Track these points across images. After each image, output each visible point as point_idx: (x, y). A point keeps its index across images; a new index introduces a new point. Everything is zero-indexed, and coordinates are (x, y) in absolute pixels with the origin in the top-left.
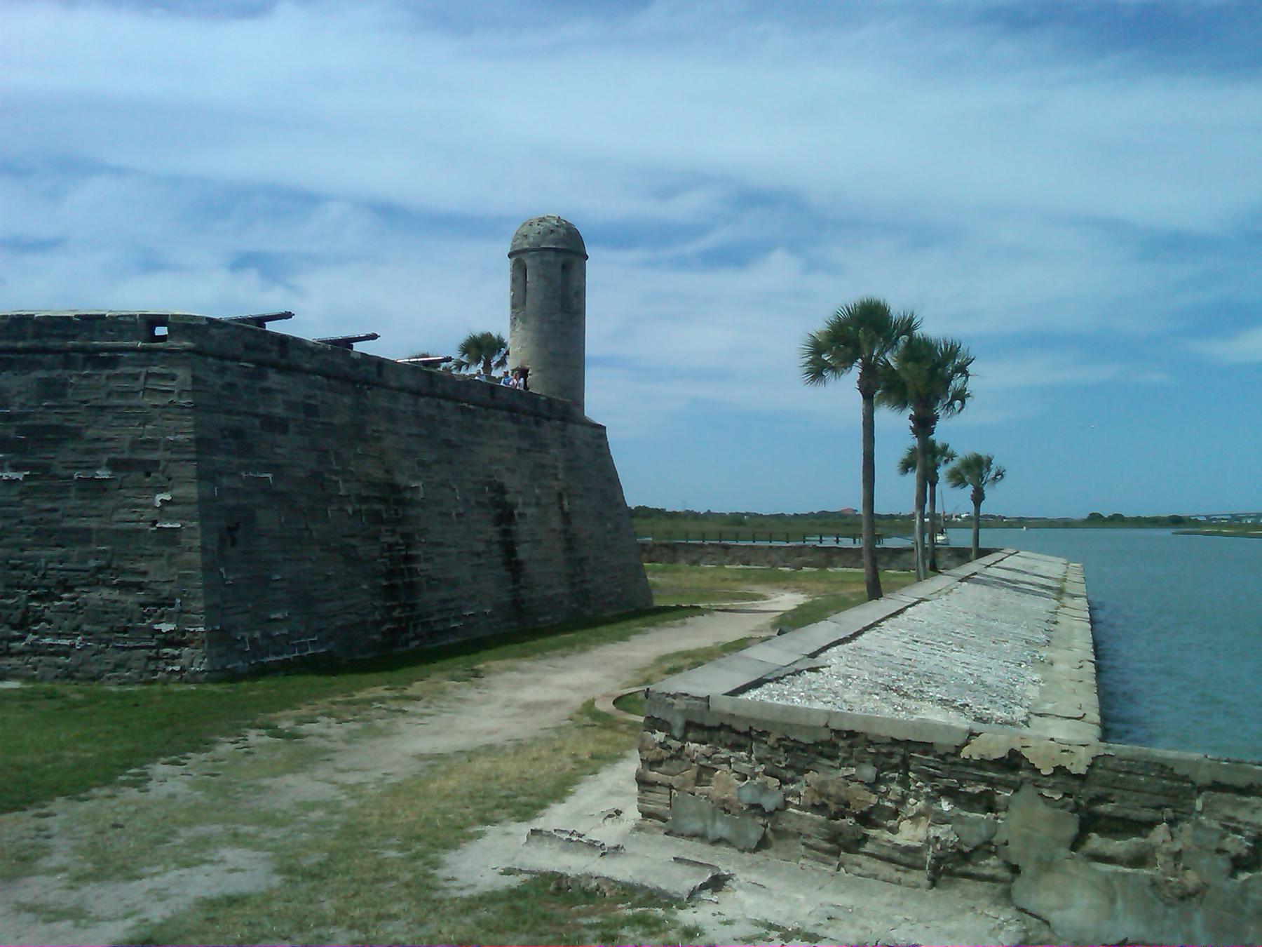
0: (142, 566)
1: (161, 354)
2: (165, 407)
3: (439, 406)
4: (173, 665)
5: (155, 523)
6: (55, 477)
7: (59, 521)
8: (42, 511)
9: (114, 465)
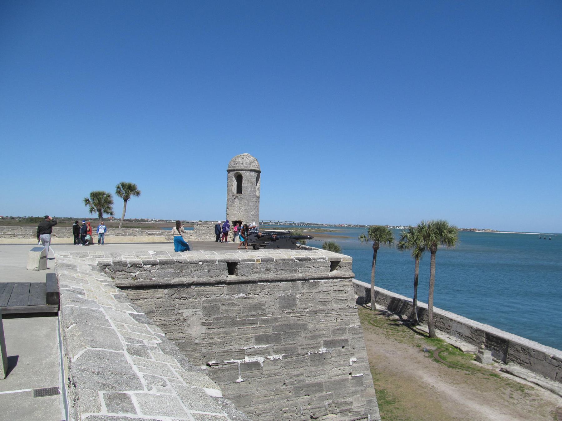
0: (350, 399)
1: (339, 279)
2: (345, 309)
6: (299, 355)
7: (303, 381)
8: (295, 376)
9: (327, 344)
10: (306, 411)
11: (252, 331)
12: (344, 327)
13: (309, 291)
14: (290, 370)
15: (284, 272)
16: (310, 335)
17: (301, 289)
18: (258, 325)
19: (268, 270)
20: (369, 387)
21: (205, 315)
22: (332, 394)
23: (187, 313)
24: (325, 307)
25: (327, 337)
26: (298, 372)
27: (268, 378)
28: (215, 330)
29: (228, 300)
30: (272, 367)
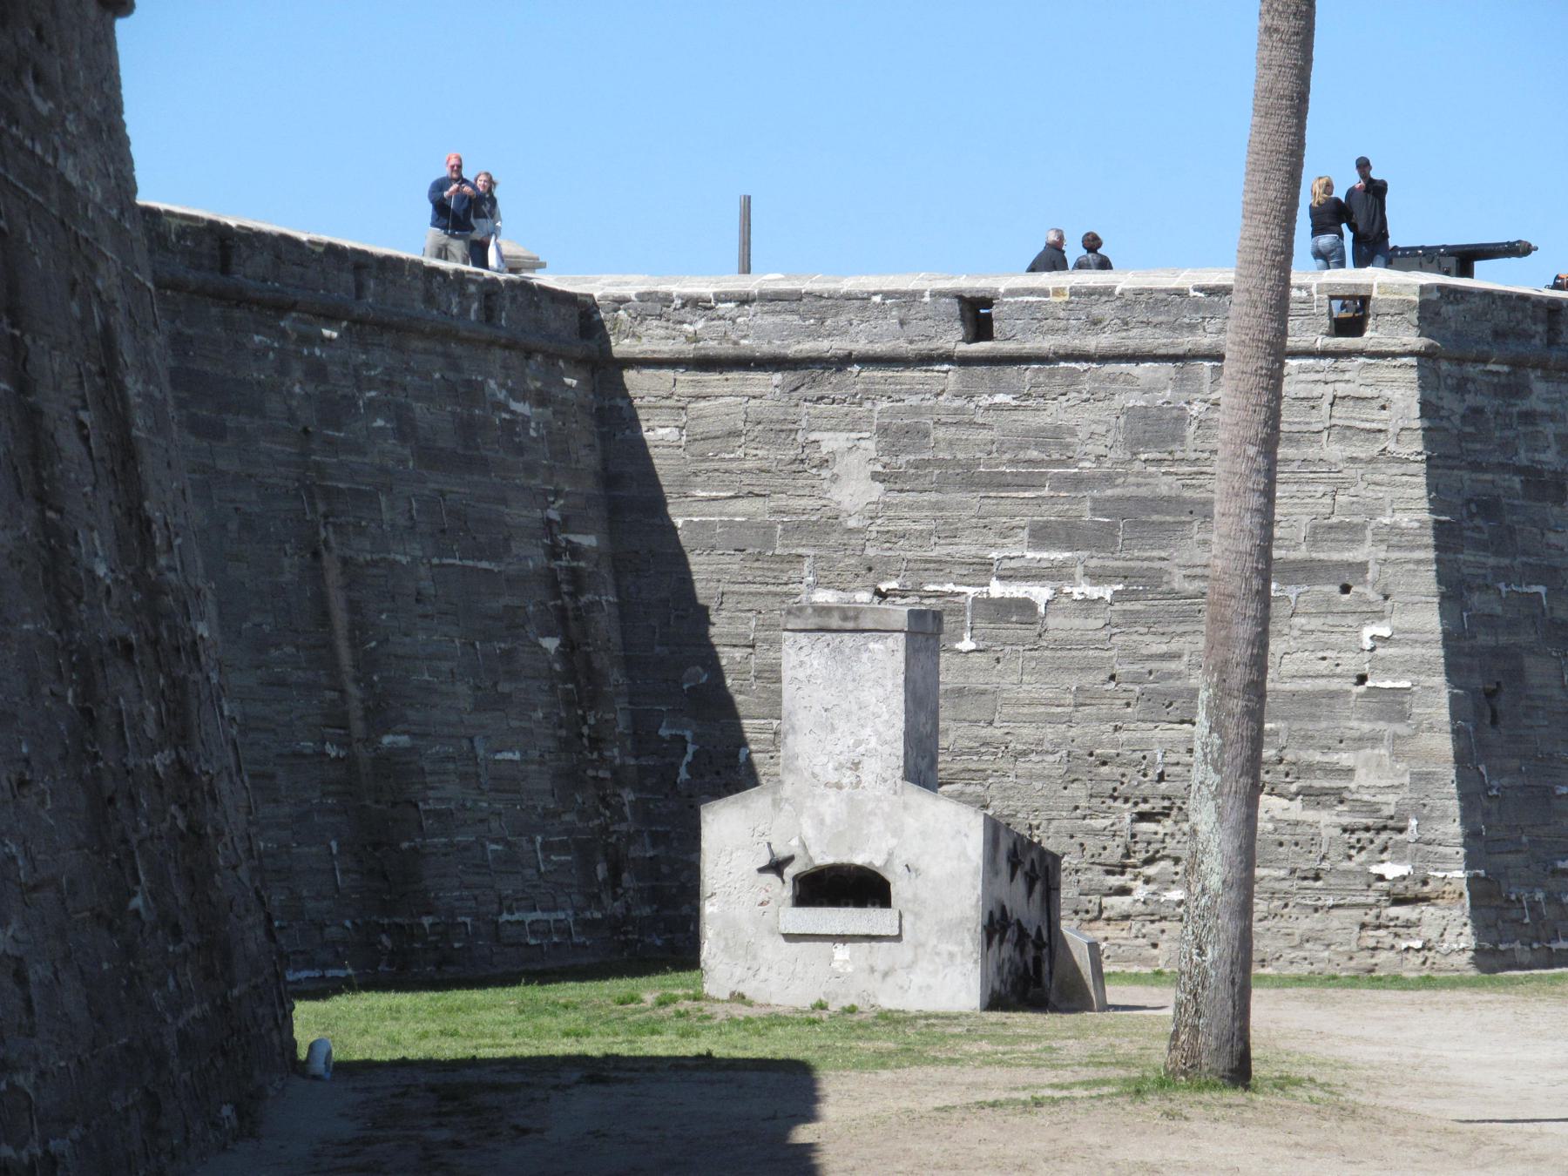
0: (1345, 759)
1: (1362, 360)
2: (1372, 460)
4: (1410, 937)
5: (1362, 679)
6: (1174, 594)
7: (1178, 675)
8: (1150, 657)
10: (1178, 769)
11: (1023, 508)
12: (1356, 520)
14: (1135, 637)
15: (1149, 331)
17: (1206, 387)
18: (1046, 492)
19: (1096, 323)
20: (1431, 728)
21: (883, 449)
23: (831, 442)
25: (1288, 548)
26: (1164, 648)
27: (1059, 654)
29: (956, 411)
30: (1077, 622)
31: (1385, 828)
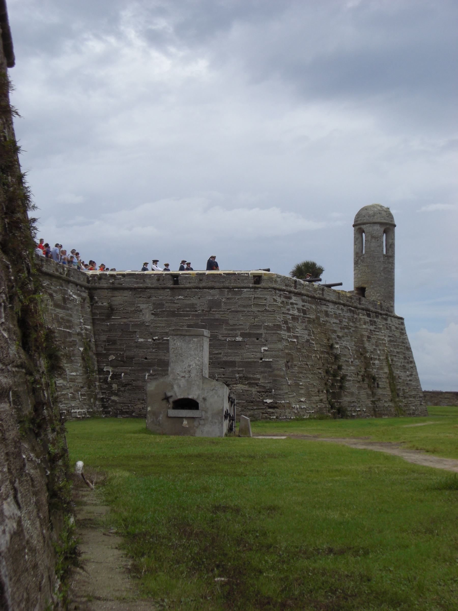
0: (258, 376)
1: (260, 290)
3: (342, 309)
4: (273, 416)
5: (261, 359)
6: (220, 340)
9: (242, 335)
10: (220, 379)
12: (260, 324)
13: (233, 297)
16: (231, 327)
18: (190, 318)
22: (242, 371)
24: (245, 309)
28: (160, 319)
29: (171, 300)
31: (267, 392)
